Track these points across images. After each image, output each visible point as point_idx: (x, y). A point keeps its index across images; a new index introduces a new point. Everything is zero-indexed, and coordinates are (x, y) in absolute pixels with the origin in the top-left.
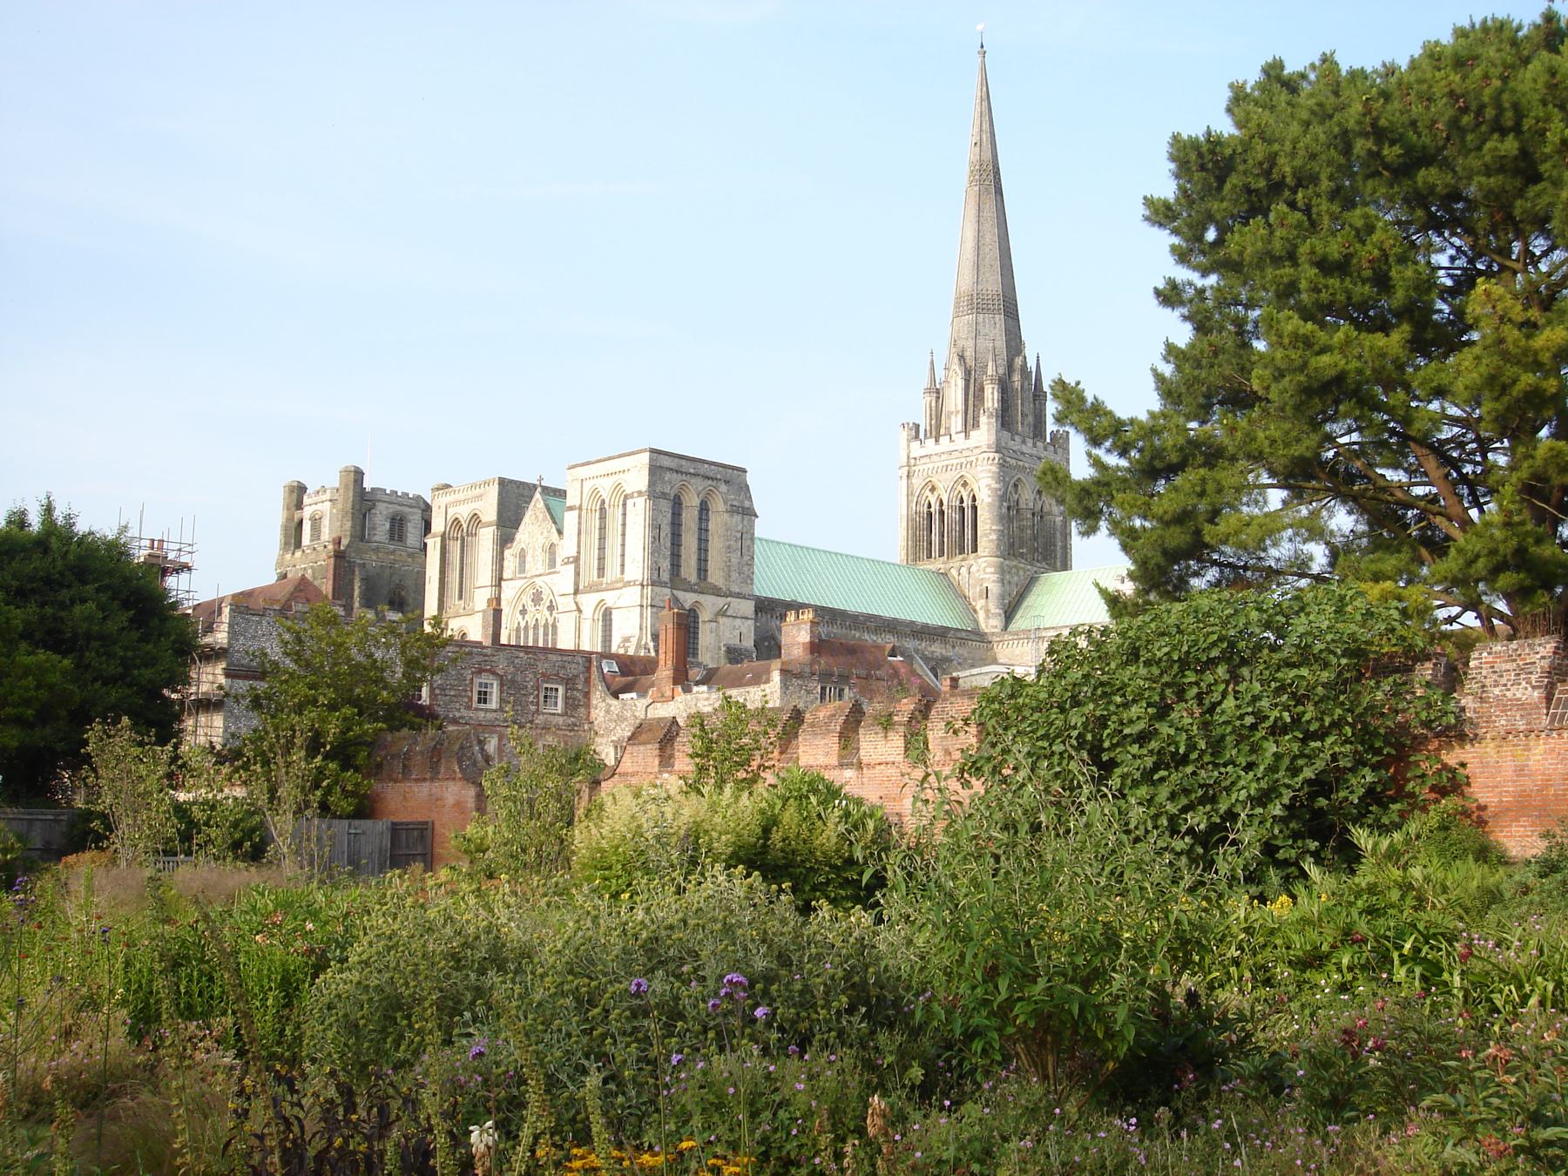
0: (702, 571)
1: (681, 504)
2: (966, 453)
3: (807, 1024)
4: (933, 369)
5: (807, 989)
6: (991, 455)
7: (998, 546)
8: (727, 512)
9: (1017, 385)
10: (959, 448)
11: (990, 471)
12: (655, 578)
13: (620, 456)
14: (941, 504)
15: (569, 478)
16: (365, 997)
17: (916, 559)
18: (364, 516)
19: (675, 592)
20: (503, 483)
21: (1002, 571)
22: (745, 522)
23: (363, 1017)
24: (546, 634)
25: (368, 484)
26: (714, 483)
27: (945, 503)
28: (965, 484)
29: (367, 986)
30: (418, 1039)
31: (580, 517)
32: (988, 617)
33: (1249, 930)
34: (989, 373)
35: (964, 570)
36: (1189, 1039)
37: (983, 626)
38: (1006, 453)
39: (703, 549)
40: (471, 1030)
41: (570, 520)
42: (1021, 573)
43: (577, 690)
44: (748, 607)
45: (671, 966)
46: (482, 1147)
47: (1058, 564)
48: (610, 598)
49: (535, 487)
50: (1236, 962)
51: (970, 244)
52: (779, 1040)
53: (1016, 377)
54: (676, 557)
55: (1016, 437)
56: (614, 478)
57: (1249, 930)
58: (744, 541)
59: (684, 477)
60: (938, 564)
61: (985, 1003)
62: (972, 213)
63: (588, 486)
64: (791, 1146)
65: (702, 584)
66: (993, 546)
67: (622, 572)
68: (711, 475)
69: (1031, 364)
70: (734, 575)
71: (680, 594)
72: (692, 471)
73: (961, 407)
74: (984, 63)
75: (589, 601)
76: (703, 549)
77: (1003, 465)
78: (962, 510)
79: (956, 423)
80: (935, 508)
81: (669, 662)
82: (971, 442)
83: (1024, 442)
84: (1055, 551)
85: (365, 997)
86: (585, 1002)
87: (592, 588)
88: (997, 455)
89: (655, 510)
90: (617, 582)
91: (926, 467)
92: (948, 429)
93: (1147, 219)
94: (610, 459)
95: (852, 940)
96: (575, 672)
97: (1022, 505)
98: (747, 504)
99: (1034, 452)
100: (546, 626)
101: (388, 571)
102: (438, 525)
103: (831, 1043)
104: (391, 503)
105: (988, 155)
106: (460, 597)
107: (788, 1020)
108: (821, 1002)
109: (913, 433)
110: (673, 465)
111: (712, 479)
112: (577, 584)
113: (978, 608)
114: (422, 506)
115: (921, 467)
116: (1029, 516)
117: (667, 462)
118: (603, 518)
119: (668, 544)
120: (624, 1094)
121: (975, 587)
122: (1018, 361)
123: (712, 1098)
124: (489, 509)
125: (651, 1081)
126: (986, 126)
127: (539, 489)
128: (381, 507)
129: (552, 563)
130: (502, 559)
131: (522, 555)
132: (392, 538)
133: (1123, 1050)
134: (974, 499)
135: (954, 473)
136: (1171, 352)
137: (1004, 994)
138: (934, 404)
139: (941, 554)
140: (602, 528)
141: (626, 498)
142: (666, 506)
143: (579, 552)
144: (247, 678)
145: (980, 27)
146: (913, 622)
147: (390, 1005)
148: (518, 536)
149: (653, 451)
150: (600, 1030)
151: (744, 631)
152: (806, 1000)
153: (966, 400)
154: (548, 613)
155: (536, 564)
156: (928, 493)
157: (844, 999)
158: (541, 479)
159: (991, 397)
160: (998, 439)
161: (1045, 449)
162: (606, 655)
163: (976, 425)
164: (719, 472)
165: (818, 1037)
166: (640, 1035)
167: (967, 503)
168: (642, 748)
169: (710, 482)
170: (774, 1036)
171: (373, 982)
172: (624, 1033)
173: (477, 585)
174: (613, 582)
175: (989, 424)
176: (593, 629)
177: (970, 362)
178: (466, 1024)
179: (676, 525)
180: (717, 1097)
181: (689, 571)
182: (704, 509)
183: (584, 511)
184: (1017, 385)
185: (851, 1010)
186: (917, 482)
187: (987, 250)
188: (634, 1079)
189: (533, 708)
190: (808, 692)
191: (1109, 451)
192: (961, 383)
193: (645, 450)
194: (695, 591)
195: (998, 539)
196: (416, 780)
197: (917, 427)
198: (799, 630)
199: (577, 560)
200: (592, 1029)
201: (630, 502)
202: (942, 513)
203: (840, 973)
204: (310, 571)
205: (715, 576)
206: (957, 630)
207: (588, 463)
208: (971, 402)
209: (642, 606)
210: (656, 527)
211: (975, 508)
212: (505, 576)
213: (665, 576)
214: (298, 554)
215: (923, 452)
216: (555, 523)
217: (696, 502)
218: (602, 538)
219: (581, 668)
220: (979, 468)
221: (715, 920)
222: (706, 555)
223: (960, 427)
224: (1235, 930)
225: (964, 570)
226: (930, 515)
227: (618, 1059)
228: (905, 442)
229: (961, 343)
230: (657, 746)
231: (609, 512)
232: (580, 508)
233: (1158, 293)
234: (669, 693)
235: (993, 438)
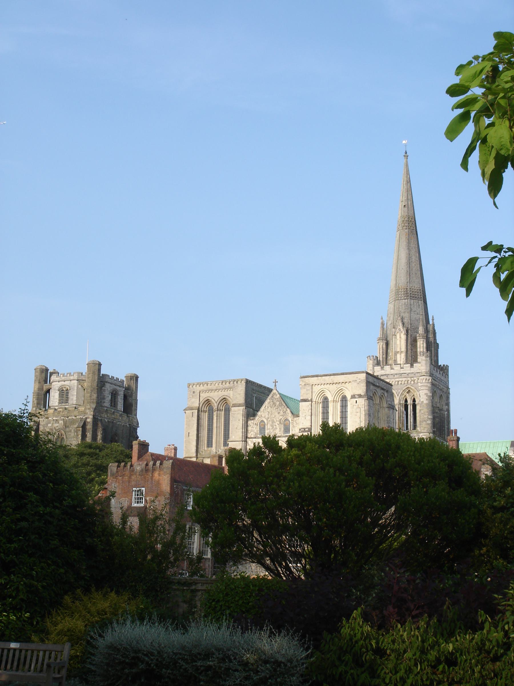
2: (410, 375)
6: (428, 378)
11: (426, 386)
20: (248, 382)
51: (403, 260)
56: (340, 385)
62: (404, 244)
63: (316, 389)
74: (407, 162)
84: (444, 430)
88: (430, 378)
94: (334, 375)
101: (111, 425)
128: (108, 386)
130: (247, 426)
134: (414, 400)
145: (404, 142)
167: (410, 402)
187: (413, 265)
192: (404, 337)
193: (363, 372)
204: (61, 422)
207: (317, 376)
211: (414, 406)
212: (249, 436)
216: (288, 407)
220: (420, 384)
228: (371, 366)
231: (331, 405)
235: (428, 368)
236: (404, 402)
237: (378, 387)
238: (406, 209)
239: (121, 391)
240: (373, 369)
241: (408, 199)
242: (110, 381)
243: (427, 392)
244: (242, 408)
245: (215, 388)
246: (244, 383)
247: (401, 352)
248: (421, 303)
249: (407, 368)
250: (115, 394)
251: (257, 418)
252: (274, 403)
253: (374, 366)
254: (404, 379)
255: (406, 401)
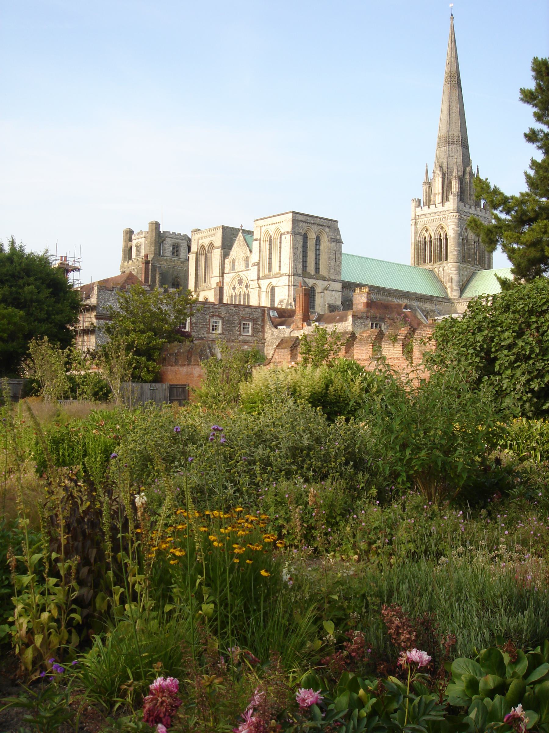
0: (317, 269)
1: (307, 237)
2: (442, 213)
3: (326, 469)
4: (427, 173)
5: (327, 454)
6: (455, 214)
7: (457, 258)
8: (329, 241)
9: (468, 180)
10: (439, 210)
11: (454, 222)
12: (295, 272)
13: (279, 215)
14: (431, 237)
15: (255, 226)
16: (134, 456)
17: (419, 263)
18: (160, 245)
19: (304, 279)
20: (224, 228)
21: (459, 269)
22: (338, 246)
23: (133, 464)
24: (244, 299)
25: (162, 229)
26: (323, 228)
27: (433, 237)
28: (442, 228)
29: (135, 451)
30: (156, 474)
31: (260, 244)
32: (452, 291)
33: (541, 434)
34: (454, 174)
35: (441, 269)
36: (500, 480)
37: (450, 295)
38: (461, 212)
39: (317, 259)
40: (178, 470)
41: (255, 245)
42: (468, 270)
43: (258, 324)
44: (339, 286)
45: (268, 443)
46: (140, 503)
47: (486, 266)
48: (274, 282)
49: (239, 230)
50: (534, 449)
51: (446, 112)
52: (313, 476)
53: (467, 177)
54: (305, 262)
55: (467, 206)
56: (276, 225)
57: (541, 434)
58: (337, 254)
59: (309, 225)
60: (429, 266)
61: (401, 460)
62: (447, 96)
63: (264, 229)
64: (312, 521)
65: (317, 276)
66: (455, 257)
67: (280, 270)
68: (321, 224)
69: (474, 170)
70: (332, 271)
71: (307, 280)
72: (312, 222)
73: (440, 191)
74: (453, 23)
75: (264, 283)
76: (317, 259)
77: (460, 219)
78: (440, 240)
79: (438, 199)
80: (428, 239)
81: (301, 312)
82: (445, 208)
83: (470, 208)
84: (485, 260)
85: (134, 456)
86: (228, 458)
87: (266, 277)
89: (295, 240)
90: (277, 274)
91: (423, 220)
92: (434, 201)
93: (521, 99)
94: (274, 216)
95: (349, 432)
96: (257, 316)
97: (469, 238)
98: (338, 237)
99: (475, 212)
100: (244, 295)
101: (171, 270)
102: (194, 248)
103: (336, 477)
104: (172, 238)
105: (454, 69)
106: (205, 282)
107: (318, 467)
108: (333, 460)
109: (418, 203)
110: (303, 219)
111: (322, 226)
112: (259, 275)
113: (447, 287)
114: (187, 239)
115: (422, 220)
116: (473, 243)
117: (300, 218)
118: (270, 244)
119: (301, 257)
120: (243, 498)
121: (446, 277)
122: (468, 169)
123: (279, 500)
124: (218, 241)
125: (255, 492)
126: (454, 54)
127: (241, 231)
128: (168, 240)
129: (247, 266)
131: (233, 262)
132: (173, 254)
133: (461, 483)
134: (446, 235)
135: (436, 223)
136: (534, 164)
137: (408, 457)
138: (427, 190)
139: (430, 261)
140: (270, 249)
141: (281, 234)
142: (300, 239)
143: (259, 260)
144: (105, 319)
145: (451, 5)
146: (416, 293)
147: (145, 458)
148: (231, 253)
149: (294, 213)
150: (234, 470)
151: (336, 297)
152: (326, 459)
153: (443, 188)
154: (245, 289)
155: (240, 265)
156: (424, 232)
157: (343, 458)
158: (242, 226)
159: (455, 186)
160: (458, 207)
161: (481, 211)
162: (272, 308)
163: (448, 200)
164: (325, 223)
165: (331, 475)
166: (252, 473)
167: (443, 237)
168: (283, 350)
169: (321, 227)
170: (311, 474)
171: (137, 449)
172: (245, 472)
173: (213, 276)
174: (275, 274)
175: (454, 199)
176: (266, 297)
177: (445, 170)
178: (176, 467)
179: (305, 247)
180: (282, 499)
181: (311, 269)
182: (318, 240)
183: (262, 241)
184: (468, 180)
185: (347, 463)
186: (419, 227)
187: (454, 115)
188: (247, 491)
189: (238, 333)
190: (365, 326)
191: (501, 212)
192: (440, 180)
194: (314, 279)
195: (457, 254)
196: (181, 366)
197: (419, 200)
198: (361, 297)
199: (258, 264)
200: (231, 469)
201: (283, 237)
202: (431, 241)
203: (343, 447)
204: (136, 270)
205: (323, 271)
206: (437, 297)
207: (264, 219)
208: (445, 189)
209: (289, 285)
210: (295, 248)
211: (446, 239)
212: (226, 272)
213: (300, 271)
214: (130, 262)
215: (422, 213)
216: (248, 247)
217: (314, 236)
218: (270, 254)
219: (260, 314)
220: (449, 221)
221: (288, 423)
222: (319, 262)
223: (440, 201)
224: (535, 434)
225: (441, 269)
226: (425, 242)
227: (241, 482)
228: (414, 207)
229: (441, 160)
230: (290, 349)
232: (260, 240)
233: (526, 135)
234: (300, 326)
235: (456, 206)
236: (439, 237)
237: (314, 224)
238: (450, 66)
239: (183, 243)
240: (415, 210)
241: (451, 57)
242: (171, 236)
243: (454, 226)
244: (219, 250)
245: (206, 235)
246: (221, 228)
247: (439, 193)
248: (459, 148)
249: (440, 208)
250: (177, 246)
251: (230, 257)
252: (240, 244)
253: (415, 207)
254: (437, 217)
255: (440, 236)
